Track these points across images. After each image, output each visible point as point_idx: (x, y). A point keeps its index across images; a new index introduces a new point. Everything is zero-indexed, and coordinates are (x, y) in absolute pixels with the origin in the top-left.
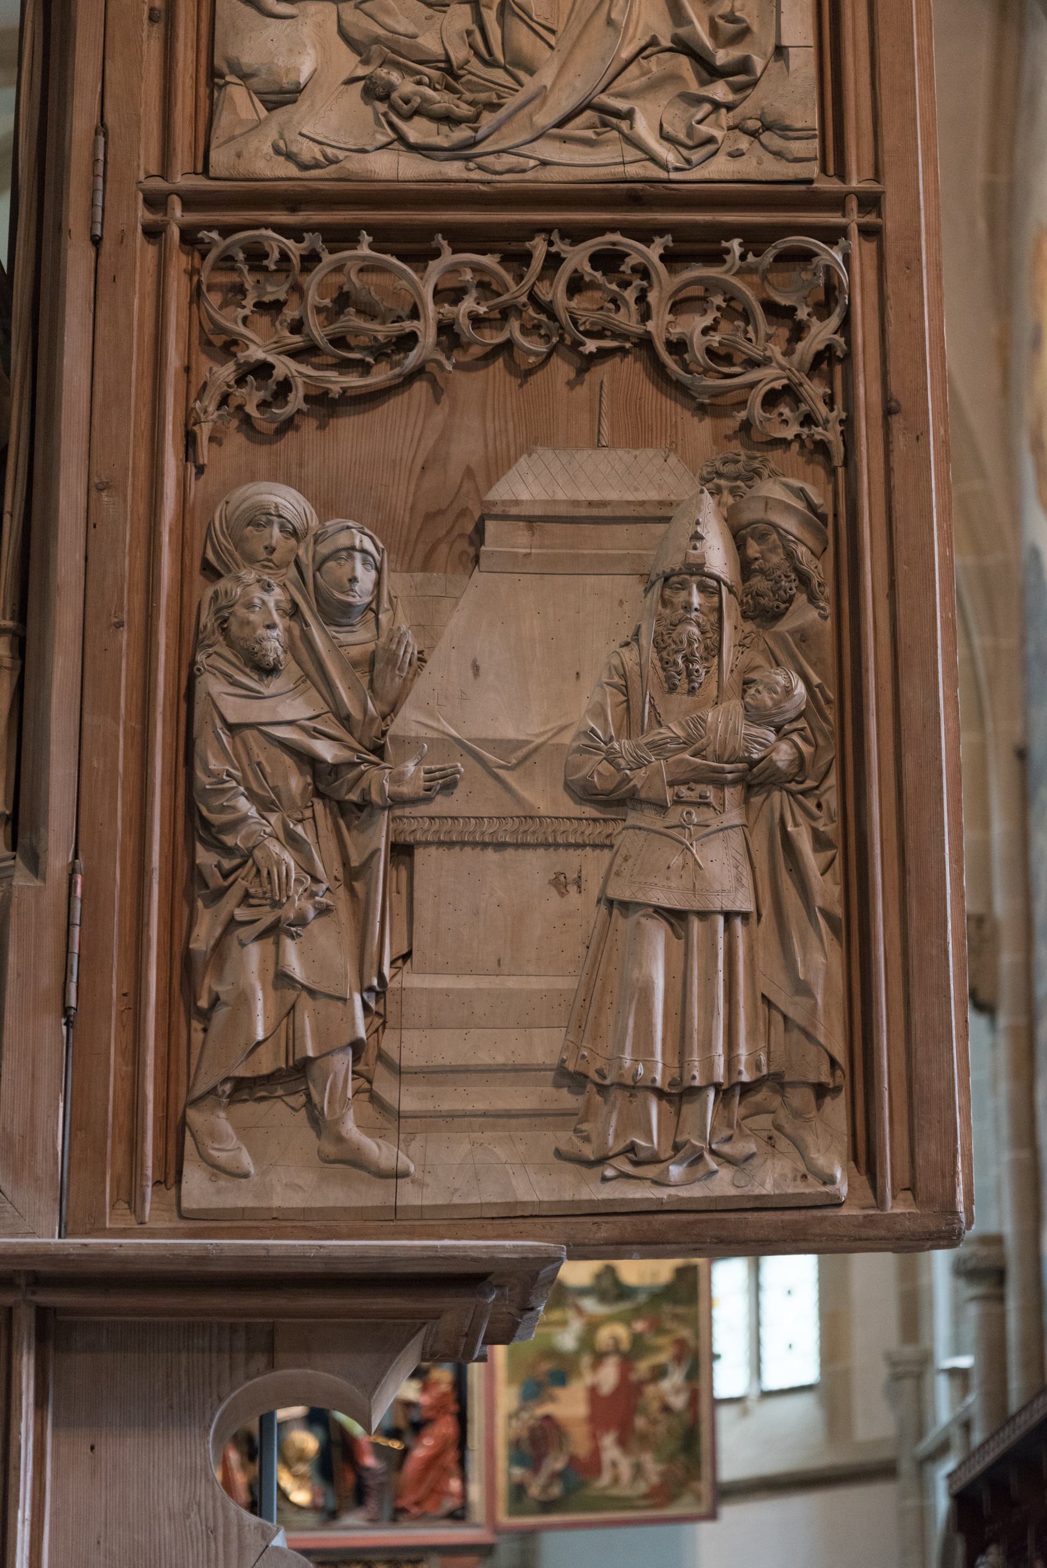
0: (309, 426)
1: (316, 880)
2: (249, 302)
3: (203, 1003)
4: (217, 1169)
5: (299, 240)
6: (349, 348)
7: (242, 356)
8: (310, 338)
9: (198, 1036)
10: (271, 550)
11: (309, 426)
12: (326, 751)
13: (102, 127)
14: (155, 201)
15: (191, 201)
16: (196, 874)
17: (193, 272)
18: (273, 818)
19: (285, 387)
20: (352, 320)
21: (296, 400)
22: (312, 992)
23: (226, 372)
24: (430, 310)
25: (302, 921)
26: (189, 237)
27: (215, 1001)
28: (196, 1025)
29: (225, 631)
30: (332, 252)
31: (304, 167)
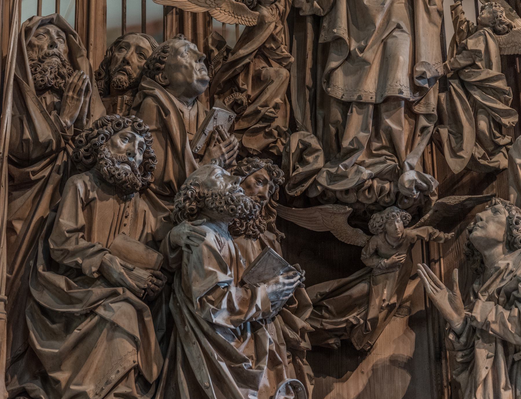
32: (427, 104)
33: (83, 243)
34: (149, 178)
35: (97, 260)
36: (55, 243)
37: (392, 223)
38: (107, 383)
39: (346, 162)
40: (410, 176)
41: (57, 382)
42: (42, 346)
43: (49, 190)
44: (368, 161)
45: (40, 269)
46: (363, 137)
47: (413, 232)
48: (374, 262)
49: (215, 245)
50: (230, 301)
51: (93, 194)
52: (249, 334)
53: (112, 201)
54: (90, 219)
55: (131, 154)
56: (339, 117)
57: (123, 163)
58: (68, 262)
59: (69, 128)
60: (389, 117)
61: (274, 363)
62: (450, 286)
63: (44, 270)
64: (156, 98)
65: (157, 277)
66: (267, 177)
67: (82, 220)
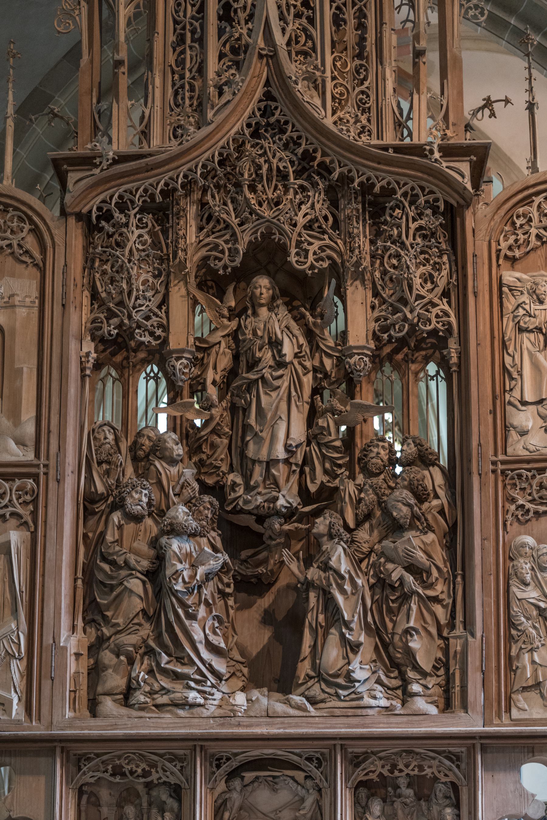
1: (541, 637)
2: (518, 488)
3: (514, 668)
4: (519, 709)
5: (530, 472)
6: (543, 499)
7: (517, 503)
8: (533, 497)
9: (513, 676)
10: (526, 553)
12: (542, 605)
13: (480, 445)
14: (494, 463)
15: (503, 462)
16: (511, 637)
17: (503, 481)
18: (530, 622)
21: (531, 514)
22: (541, 665)
23: (513, 507)
25: (538, 648)
27: (517, 668)
28: (512, 673)
29: (516, 575)
30: (539, 475)
31: (531, 452)
32: (296, 458)
33: (117, 548)
34: (152, 509)
35: (123, 558)
36: (104, 548)
37: (273, 525)
38: (128, 619)
39: (251, 494)
40: (281, 502)
41: (108, 617)
42: (100, 599)
43: (104, 518)
44: (264, 491)
45: (98, 562)
46: (260, 479)
51: (122, 522)
52: (196, 591)
53: (132, 524)
54: (121, 536)
56: (251, 466)
57: (137, 505)
58: (110, 558)
59: (113, 484)
60: (273, 468)
62: (298, 559)
63: (100, 562)
64: (155, 466)
65: (154, 563)
66: (209, 507)
67: (117, 537)
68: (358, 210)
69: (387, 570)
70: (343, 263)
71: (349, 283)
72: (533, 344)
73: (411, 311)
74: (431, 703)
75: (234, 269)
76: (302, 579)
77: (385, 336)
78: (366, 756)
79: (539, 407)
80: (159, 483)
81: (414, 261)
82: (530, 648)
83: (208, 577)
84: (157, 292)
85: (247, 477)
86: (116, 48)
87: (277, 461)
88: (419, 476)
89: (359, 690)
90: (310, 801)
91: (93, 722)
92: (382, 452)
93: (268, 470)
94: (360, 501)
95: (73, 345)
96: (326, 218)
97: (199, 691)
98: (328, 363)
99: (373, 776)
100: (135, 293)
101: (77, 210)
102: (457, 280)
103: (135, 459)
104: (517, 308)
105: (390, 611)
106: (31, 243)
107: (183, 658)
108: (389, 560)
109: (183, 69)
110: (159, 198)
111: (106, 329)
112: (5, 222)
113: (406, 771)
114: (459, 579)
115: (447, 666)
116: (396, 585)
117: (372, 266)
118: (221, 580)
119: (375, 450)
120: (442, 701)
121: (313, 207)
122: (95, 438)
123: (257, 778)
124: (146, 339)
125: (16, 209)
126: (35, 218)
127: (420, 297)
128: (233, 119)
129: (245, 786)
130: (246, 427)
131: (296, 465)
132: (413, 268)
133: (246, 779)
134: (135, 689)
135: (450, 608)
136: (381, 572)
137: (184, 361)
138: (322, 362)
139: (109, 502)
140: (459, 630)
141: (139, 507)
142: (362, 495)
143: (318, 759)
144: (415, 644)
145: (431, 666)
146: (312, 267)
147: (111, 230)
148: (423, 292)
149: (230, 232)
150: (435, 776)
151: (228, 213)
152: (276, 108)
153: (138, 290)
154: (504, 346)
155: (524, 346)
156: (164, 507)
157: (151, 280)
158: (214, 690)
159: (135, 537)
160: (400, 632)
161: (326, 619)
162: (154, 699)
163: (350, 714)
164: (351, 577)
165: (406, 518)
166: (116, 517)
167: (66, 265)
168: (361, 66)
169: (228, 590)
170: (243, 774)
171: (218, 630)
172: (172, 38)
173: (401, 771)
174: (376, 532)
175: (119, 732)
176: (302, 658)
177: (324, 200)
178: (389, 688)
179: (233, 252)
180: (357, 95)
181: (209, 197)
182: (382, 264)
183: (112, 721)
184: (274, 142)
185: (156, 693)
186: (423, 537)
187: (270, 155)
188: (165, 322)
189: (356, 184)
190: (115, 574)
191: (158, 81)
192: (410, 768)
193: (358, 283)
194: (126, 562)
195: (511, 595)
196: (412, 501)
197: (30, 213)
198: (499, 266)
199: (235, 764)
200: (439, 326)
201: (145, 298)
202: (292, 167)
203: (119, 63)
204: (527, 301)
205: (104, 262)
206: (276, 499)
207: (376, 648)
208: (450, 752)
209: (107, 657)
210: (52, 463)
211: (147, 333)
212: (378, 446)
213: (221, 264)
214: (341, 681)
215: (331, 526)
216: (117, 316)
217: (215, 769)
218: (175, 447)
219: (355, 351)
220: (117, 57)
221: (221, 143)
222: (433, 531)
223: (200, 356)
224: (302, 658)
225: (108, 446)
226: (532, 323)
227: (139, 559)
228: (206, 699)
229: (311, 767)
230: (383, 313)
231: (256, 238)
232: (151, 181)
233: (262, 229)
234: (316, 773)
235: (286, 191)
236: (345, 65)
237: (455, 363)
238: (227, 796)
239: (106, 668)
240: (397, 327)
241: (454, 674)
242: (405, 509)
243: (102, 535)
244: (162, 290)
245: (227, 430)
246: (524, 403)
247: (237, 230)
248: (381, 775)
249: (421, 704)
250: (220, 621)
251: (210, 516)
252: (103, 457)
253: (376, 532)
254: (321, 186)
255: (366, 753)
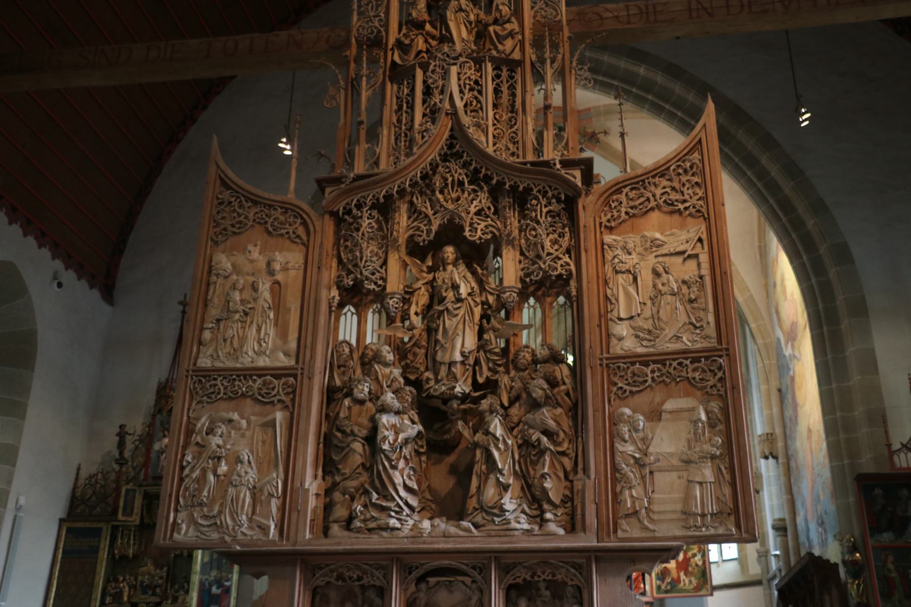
0: (630, 397)
11: (630, 397)
12: (637, 455)
13: (591, 347)
14: (601, 359)
15: (607, 359)
16: (616, 478)
17: (608, 371)
19: (625, 391)
20: (636, 378)
21: (628, 393)
23: (615, 389)
24: (650, 375)
26: (607, 365)
27: (621, 500)
33: (347, 422)
35: (350, 428)
40: (458, 389)
45: (334, 431)
47: (462, 407)
48: (451, 417)
49: (385, 423)
50: (389, 441)
51: (351, 405)
52: (398, 450)
53: (358, 406)
55: (363, 390)
61: (405, 458)
62: (469, 428)
68: (509, 202)
69: (529, 434)
70: (500, 235)
71: (504, 247)
72: (625, 281)
73: (544, 263)
74: (560, 526)
75: (429, 241)
76: (472, 441)
77: (528, 280)
78: (514, 565)
79: (631, 321)
80: (377, 379)
81: (545, 232)
82: (629, 485)
83: (406, 441)
84: (380, 258)
85: (436, 374)
86: (359, 115)
87: (456, 362)
88: (551, 370)
89: (509, 517)
90: (475, 598)
91: (324, 541)
92: (527, 355)
93: (449, 368)
94: (512, 388)
95: (324, 293)
96: (489, 208)
97: (398, 519)
98: (491, 299)
99: (519, 580)
100: (364, 259)
101: (330, 209)
102: (575, 243)
103: (363, 364)
104: (614, 258)
105: (532, 462)
106: (301, 231)
107: (387, 496)
108: (531, 427)
109: (401, 124)
110: (382, 200)
111: (346, 281)
112: (285, 219)
113: (543, 577)
114: (580, 439)
115: (572, 500)
116: (536, 444)
117: (520, 236)
118: (416, 443)
119: (522, 354)
120: (569, 527)
121: (480, 202)
122: (337, 351)
123: (438, 582)
124: (372, 287)
125: (292, 210)
126: (304, 216)
127: (549, 254)
128: (429, 152)
129: (430, 588)
130: (437, 341)
131: (469, 365)
132: (544, 237)
133: (430, 583)
134: (354, 518)
135: (573, 459)
136: (526, 436)
137: (395, 300)
138: (487, 298)
139: (344, 392)
140: (580, 474)
141: (362, 395)
142: (513, 384)
143: (480, 568)
144: (548, 484)
145: (560, 500)
146: (480, 238)
147: (351, 220)
148: (552, 251)
149: (427, 219)
150: (564, 581)
151: (426, 208)
152: (457, 144)
153: (367, 257)
154: (606, 283)
155: (619, 282)
156: (379, 394)
157: (376, 250)
158: (408, 518)
159: (360, 415)
160: (538, 476)
161: (487, 468)
162: (366, 525)
163: (502, 534)
164: (504, 440)
165: (541, 397)
166: (347, 402)
167: (322, 243)
168: (512, 117)
169: (421, 450)
170: (428, 579)
171: (412, 477)
172: (395, 107)
173: (539, 576)
174: (523, 409)
175: (341, 548)
176: (470, 495)
177: (488, 198)
178: (530, 516)
179: (429, 232)
180: (510, 134)
181: (414, 199)
182: (525, 235)
183: (338, 540)
184: (456, 164)
185: (368, 520)
186: (554, 411)
187: (453, 172)
188: (384, 276)
189: (507, 186)
190: (344, 440)
191: (385, 132)
192: (546, 574)
193: (510, 247)
194: (352, 431)
195: (615, 450)
196: (546, 386)
197: (301, 213)
198: (601, 233)
199: (420, 572)
200: (563, 272)
201: (371, 261)
202: (467, 178)
203: (361, 123)
204: (620, 254)
205: (346, 240)
206: (455, 387)
207: (522, 488)
208: (574, 563)
209: (337, 496)
210: (306, 367)
211: (372, 284)
212: (524, 351)
213: (421, 239)
214: (496, 511)
215: (491, 405)
216: (353, 273)
217: (407, 575)
218: (388, 355)
219: (507, 290)
220: (359, 119)
221: (421, 166)
222: (561, 407)
223: (407, 297)
224: (470, 495)
225: (345, 356)
226: (624, 267)
227: (361, 429)
228: (402, 524)
229: (476, 574)
230: (527, 265)
231: (444, 222)
232: (377, 190)
233: (448, 217)
234: (479, 578)
235: (463, 192)
236: (501, 116)
237: (575, 296)
238: (416, 595)
239: (336, 504)
240: (535, 274)
241: (576, 506)
242: (540, 392)
243: (338, 413)
244: (383, 256)
245: (424, 343)
246: (620, 319)
247: (432, 218)
248: (525, 579)
249: (552, 527)
250: (414, 470)
251: (410, 400)
252: (342, 362)
253: (523, 409)
254: (486, 189)
255: (515, 563)
